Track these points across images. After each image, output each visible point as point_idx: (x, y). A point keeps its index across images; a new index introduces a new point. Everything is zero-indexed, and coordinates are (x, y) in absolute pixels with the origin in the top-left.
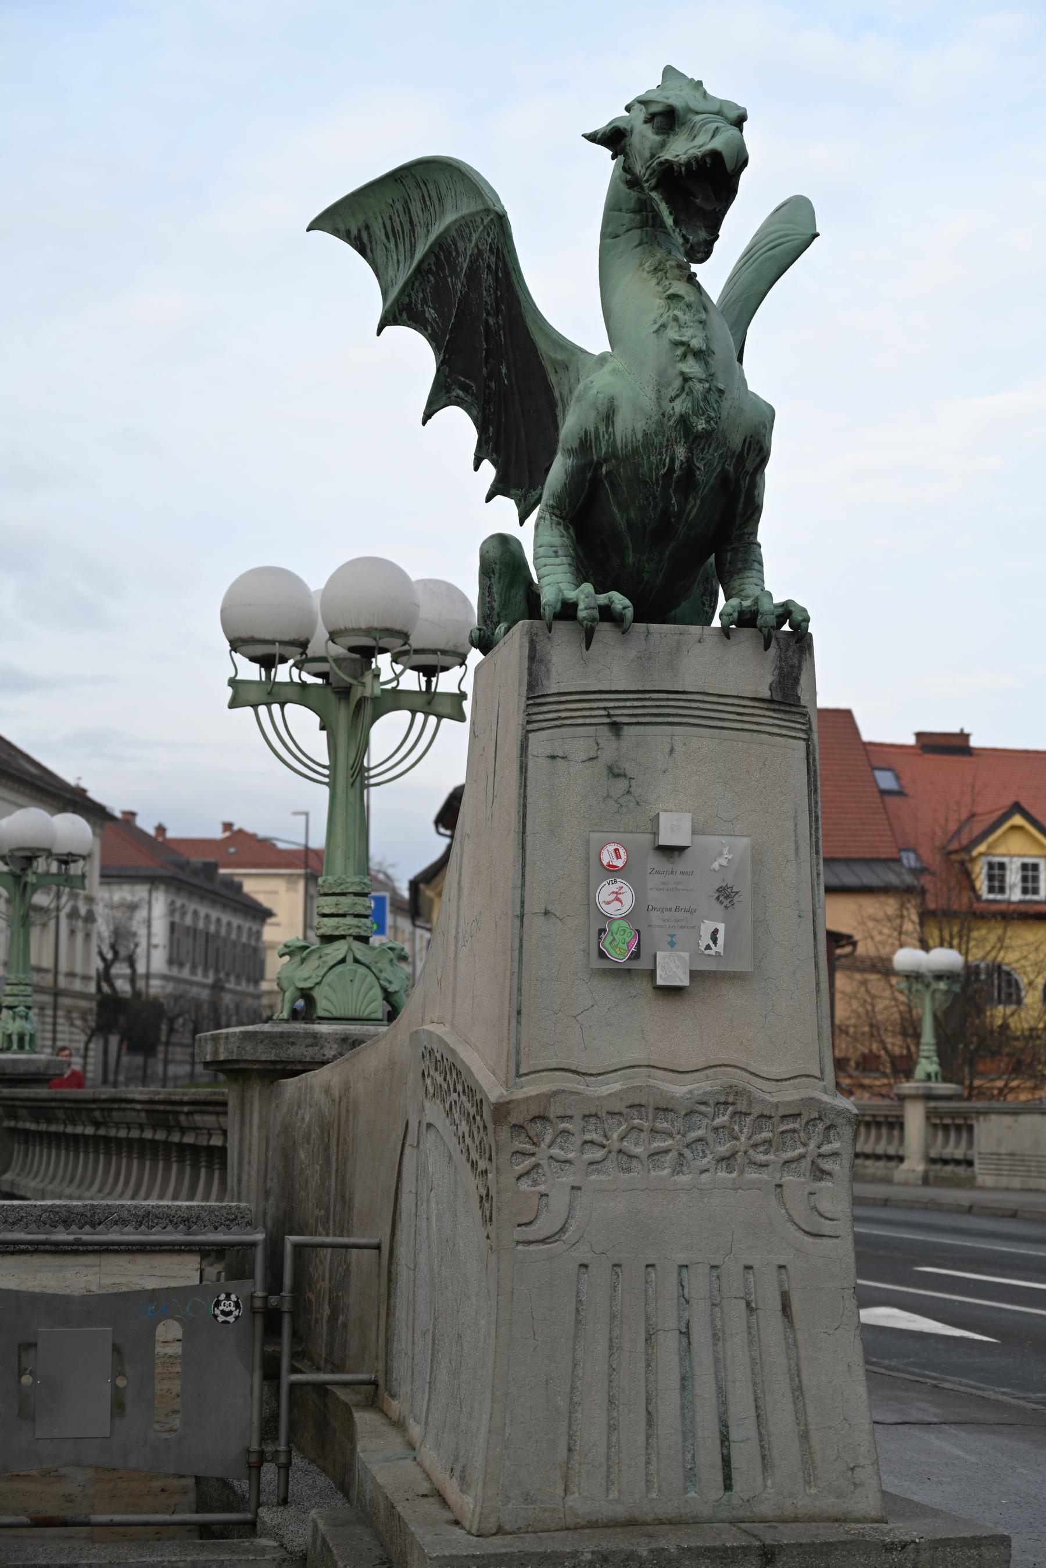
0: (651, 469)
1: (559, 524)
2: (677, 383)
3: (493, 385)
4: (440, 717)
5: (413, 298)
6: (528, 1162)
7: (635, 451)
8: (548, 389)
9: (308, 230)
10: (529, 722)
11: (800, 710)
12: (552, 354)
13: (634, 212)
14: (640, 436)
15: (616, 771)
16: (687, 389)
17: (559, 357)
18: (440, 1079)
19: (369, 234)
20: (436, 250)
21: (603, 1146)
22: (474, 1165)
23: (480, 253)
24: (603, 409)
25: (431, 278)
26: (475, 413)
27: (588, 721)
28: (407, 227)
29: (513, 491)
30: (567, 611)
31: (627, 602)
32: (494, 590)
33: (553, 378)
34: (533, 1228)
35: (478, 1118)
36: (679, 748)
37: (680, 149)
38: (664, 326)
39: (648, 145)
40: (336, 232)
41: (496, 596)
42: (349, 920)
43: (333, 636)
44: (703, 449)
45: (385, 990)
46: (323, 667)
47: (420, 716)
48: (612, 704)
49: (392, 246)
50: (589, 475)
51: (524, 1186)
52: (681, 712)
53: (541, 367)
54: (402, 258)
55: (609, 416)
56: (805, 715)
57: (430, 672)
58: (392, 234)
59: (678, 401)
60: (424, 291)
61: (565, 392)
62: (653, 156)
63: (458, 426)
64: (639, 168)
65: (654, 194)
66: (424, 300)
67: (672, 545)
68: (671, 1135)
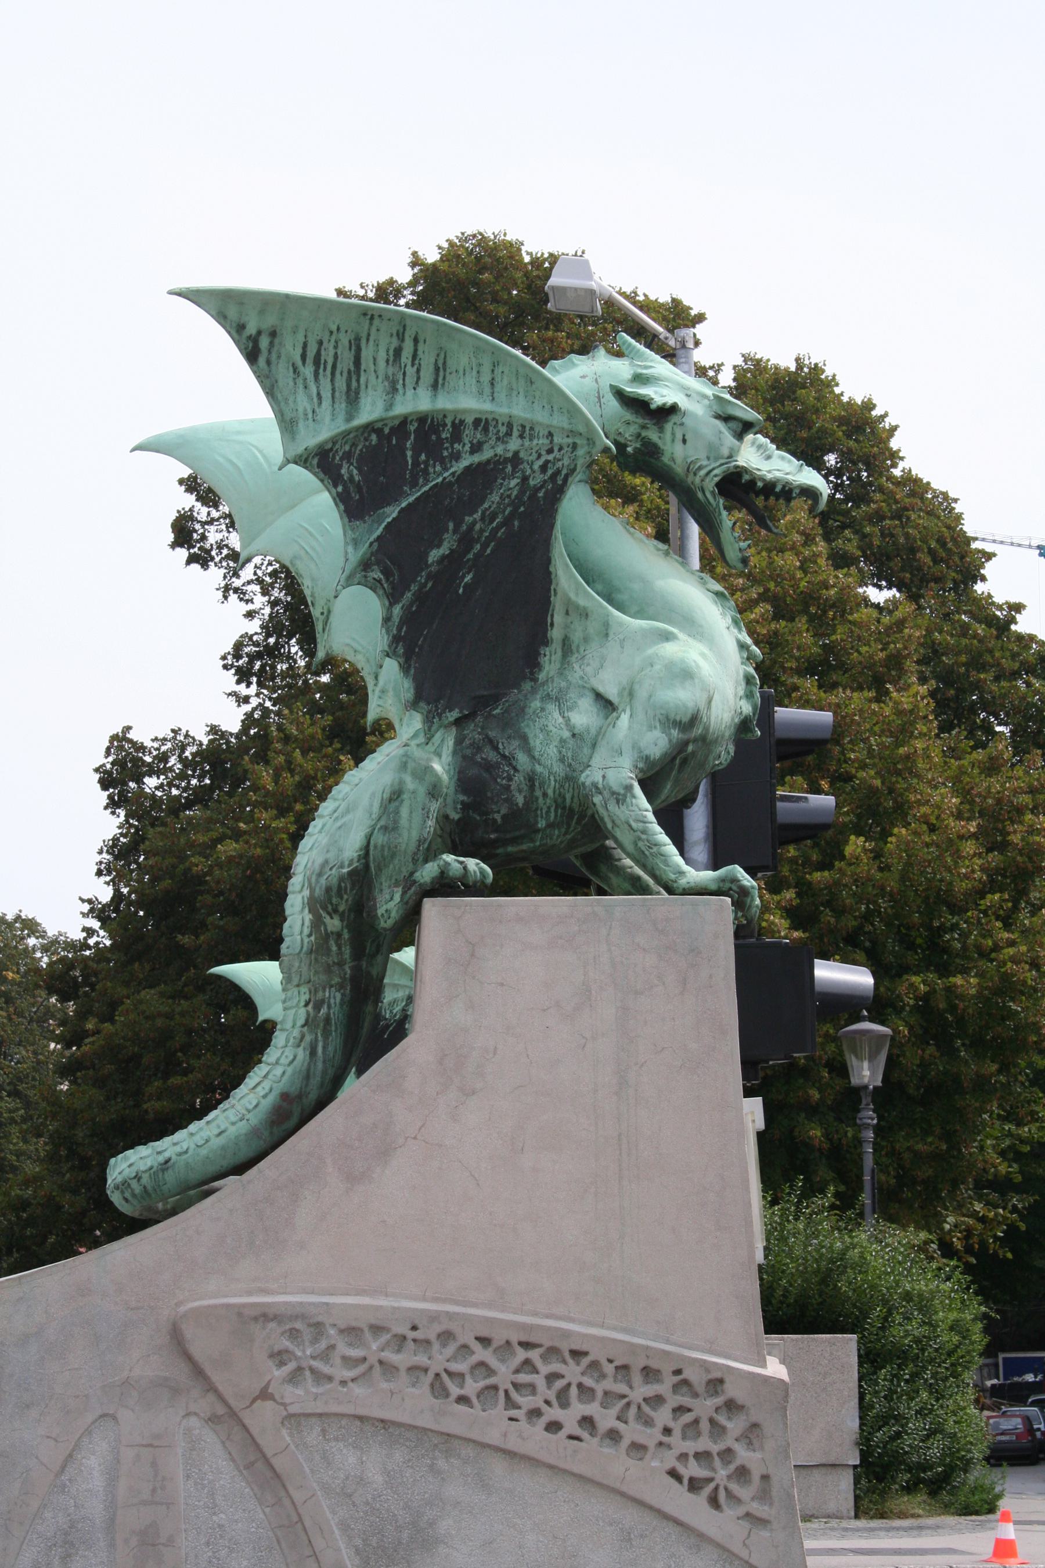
5: (337, 446)
12: (572, 596)
17: (582, 602)
19: (271, 344)
23: (516, 460)
25: (374, 437)
26: (387, 603)
33: (558, 618)
40: (221, 318)
49: (308, 371)
53: (548, 602)
54: (326, 394)
60: (354, 445)
61: (576, 637)
62: (730, 457)
66: (348, 456)
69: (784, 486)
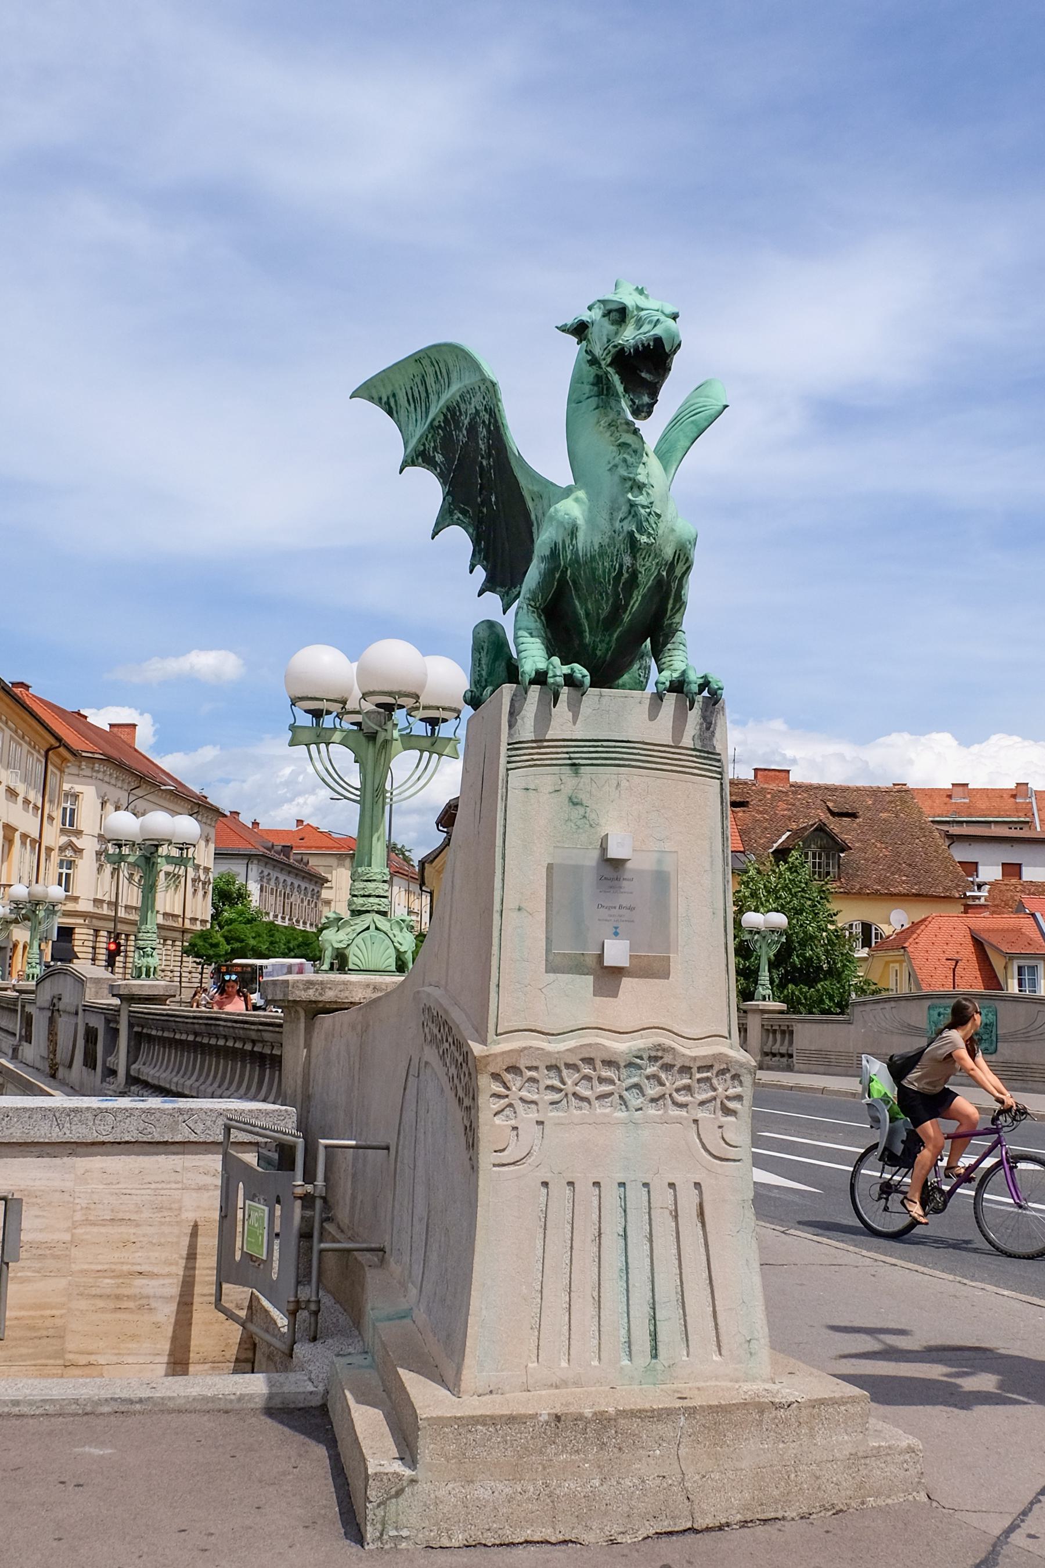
0: (604, 571)
1: (533, 612)
2: (625, 508)
3: (485, 510)
4: (440, 755)
6: (504, 1102)
7: (593, 558)
8: (526, 513)
9: (351, 398)
10: (509, 762)
11: (718, 757)
12: (530, 487)
13: (593, 384)
14: (596, 547)
15: (575, 800)
16: (633, 513)
18: (436, 1031)
19: (396, 401)
20: (445, 410)
21: (561, 1090)
22: (460, 1101)
23: (477, 412)
24: (569, 527)
27: (554, 762)
28: (423, 395)
29: (498, 589)
30: (540, 678)
31: (585, 672)
32: (483, 662)
33: (530, 504)
34: (506, 1153)
35: (464, 1065)
36: (624, 784)
37: (629, 336)
38: (616, 466)
39: (605, 333)
40: (371, 399)
41: (484, 667)
42: (372, 900)
43: (365, 696)
44: (644, 559)
45: (397, 950)
46: (359, 718)
47: (426, 754)
48: (572, 750)
50: (557, 576)
51: (498, 1121)
52: (625, 756)
54: (419, 418)
55: (573, 532)
56: (719, 761)
57: (433, 722)
58: (412, 400)
59: (626, 522)
61: (540, 515)
62: (609, 341)
63: (459, 539)
64: (598, 351)
65: (609, 369)
66: (435, 449)
67: (619, 630)
68: (611, 1082)
69: (643, 345)
